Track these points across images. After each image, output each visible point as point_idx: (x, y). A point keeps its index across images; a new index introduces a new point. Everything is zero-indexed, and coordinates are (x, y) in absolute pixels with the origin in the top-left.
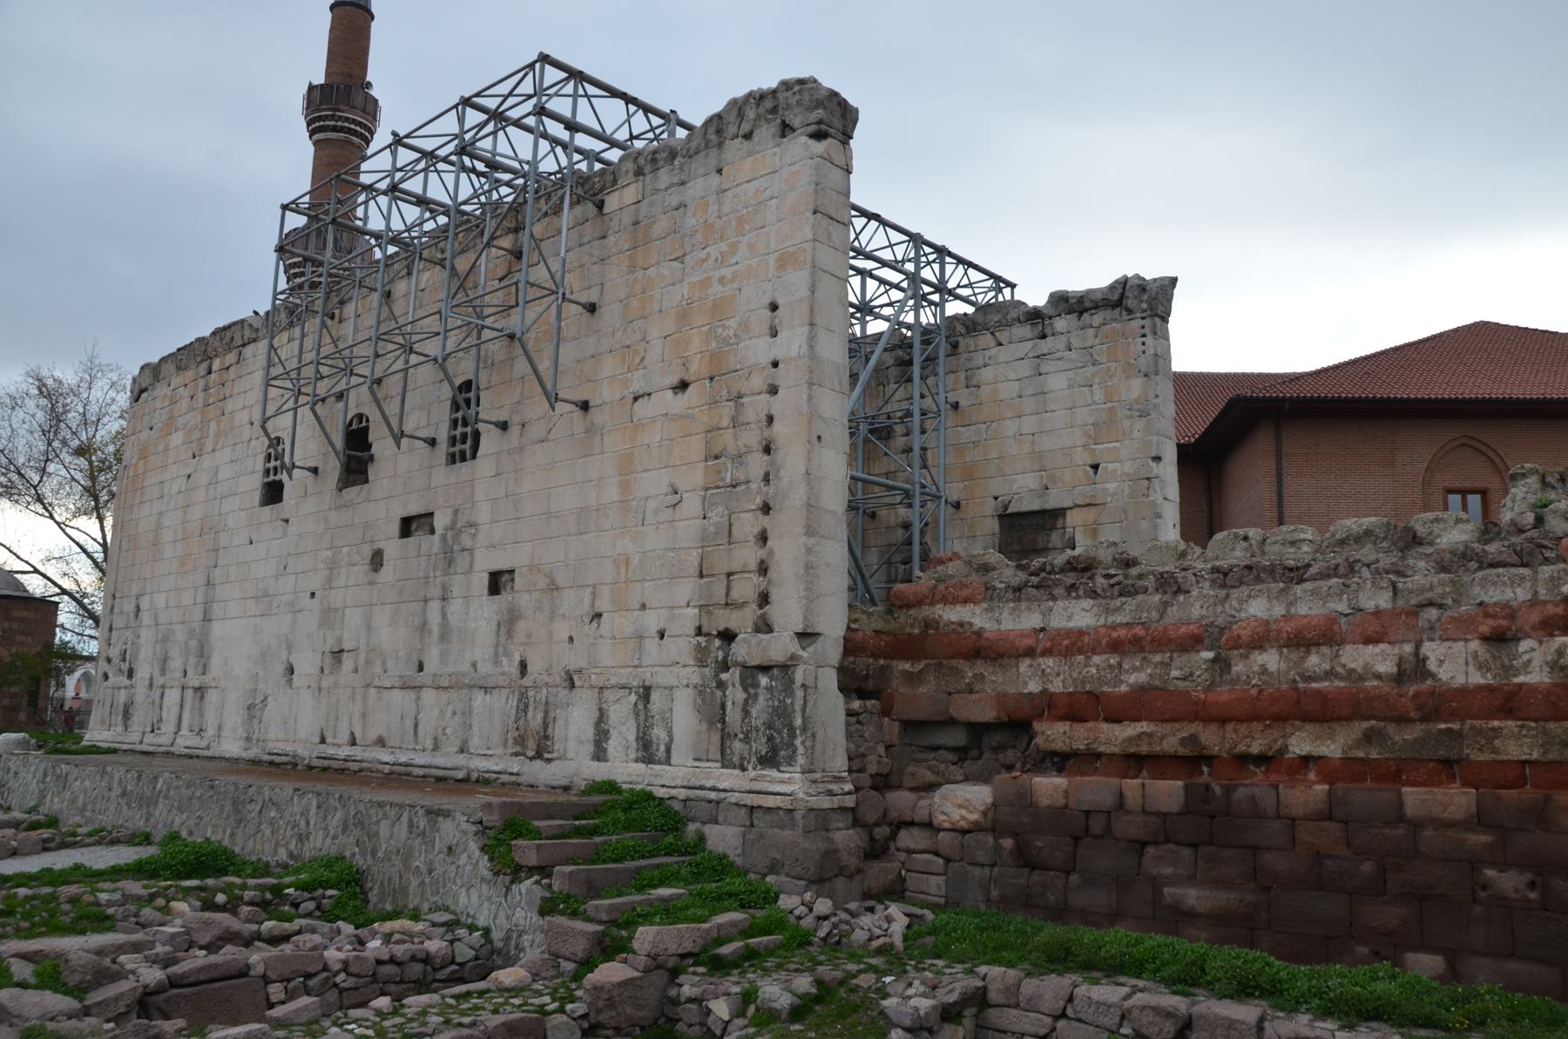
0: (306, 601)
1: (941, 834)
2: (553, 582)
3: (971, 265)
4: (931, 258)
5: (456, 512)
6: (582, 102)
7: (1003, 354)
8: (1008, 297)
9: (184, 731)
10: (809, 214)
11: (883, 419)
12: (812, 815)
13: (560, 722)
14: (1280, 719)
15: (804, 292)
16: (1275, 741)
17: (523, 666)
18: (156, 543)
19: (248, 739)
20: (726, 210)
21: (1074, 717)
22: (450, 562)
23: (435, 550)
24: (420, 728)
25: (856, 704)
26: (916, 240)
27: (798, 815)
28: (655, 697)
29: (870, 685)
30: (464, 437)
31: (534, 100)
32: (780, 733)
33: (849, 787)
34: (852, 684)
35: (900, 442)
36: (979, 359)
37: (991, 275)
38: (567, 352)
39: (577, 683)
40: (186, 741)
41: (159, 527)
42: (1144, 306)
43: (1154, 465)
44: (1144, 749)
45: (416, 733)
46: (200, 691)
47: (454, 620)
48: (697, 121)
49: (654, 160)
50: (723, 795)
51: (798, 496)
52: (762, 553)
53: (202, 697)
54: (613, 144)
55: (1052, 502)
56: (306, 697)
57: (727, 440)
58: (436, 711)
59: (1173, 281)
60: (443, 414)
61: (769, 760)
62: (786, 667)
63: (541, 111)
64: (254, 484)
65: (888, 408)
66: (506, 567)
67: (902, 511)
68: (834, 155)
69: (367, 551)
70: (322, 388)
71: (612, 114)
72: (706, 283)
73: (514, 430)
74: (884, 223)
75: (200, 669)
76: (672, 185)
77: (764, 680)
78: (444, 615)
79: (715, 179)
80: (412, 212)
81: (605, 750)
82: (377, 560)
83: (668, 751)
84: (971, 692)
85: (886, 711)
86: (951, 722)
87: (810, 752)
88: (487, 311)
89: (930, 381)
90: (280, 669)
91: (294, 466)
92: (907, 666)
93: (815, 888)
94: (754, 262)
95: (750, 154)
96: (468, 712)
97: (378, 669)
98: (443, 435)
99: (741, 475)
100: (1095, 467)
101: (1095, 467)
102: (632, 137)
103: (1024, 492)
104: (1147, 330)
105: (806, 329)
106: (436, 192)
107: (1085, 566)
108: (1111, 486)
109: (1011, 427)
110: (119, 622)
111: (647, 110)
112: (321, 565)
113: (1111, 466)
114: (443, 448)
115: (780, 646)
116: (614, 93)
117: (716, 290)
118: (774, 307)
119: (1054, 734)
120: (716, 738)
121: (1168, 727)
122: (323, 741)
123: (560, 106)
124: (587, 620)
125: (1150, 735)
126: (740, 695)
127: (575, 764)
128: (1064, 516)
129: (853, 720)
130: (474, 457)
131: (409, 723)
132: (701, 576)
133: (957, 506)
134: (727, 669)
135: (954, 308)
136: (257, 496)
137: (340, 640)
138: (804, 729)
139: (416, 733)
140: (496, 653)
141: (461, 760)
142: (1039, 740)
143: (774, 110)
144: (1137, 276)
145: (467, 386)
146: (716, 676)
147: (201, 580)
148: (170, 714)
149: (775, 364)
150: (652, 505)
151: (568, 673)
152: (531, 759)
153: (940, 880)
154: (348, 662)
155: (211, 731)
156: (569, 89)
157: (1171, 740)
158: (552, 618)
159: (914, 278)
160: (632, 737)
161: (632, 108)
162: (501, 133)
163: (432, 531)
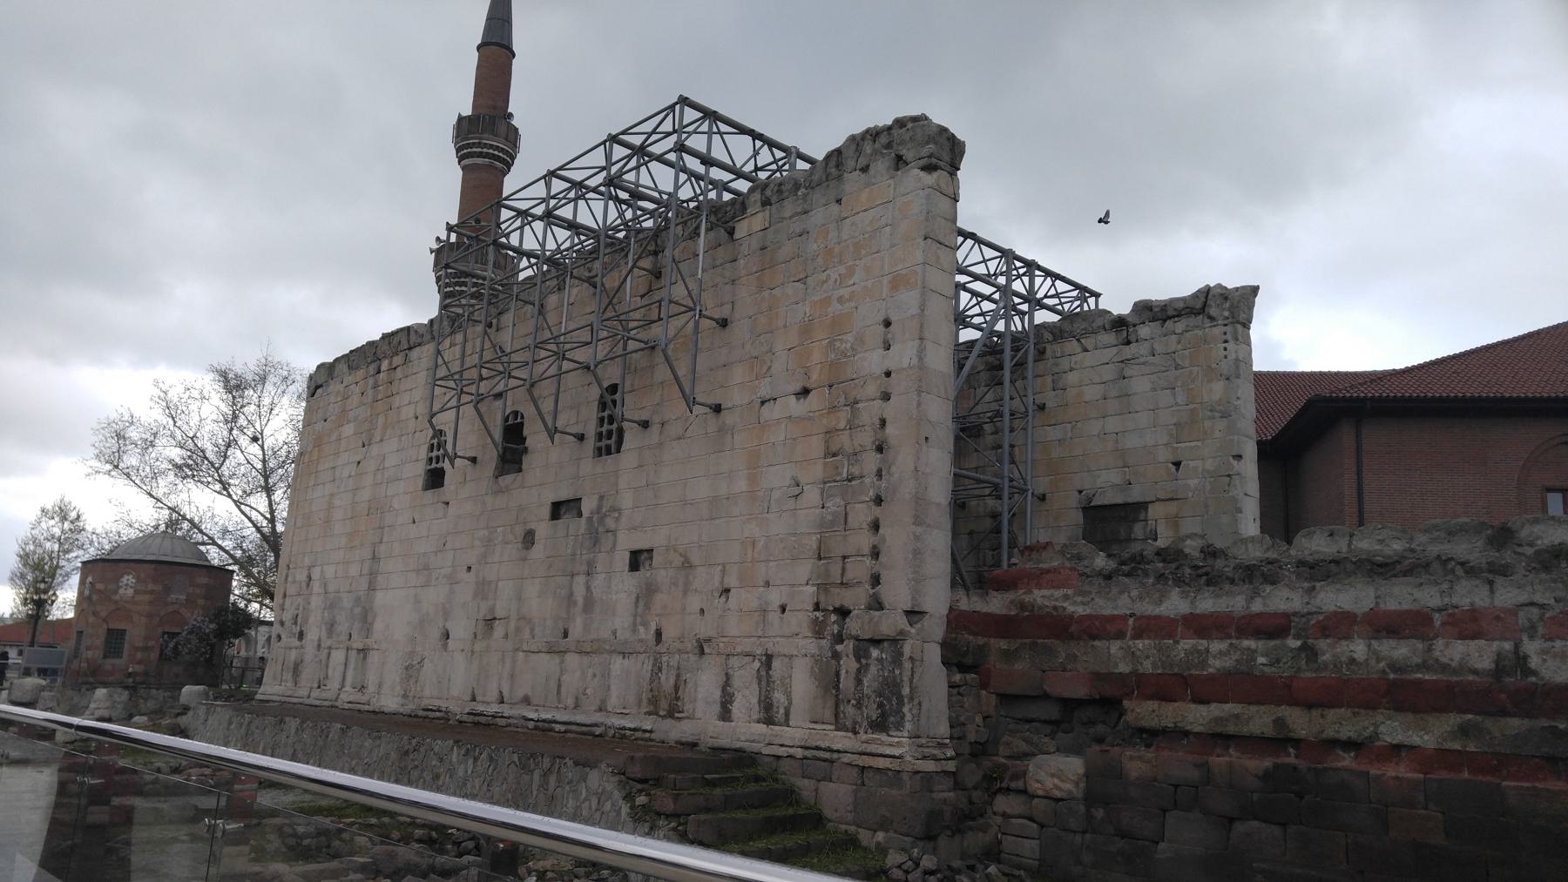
0: (463, 575)
1: (1036, 800)
2: (687, 560)
3: (1057, 277)
4: (1022, 271)
5: (601, 498)
6: (716, 138)
7: (1089, 359)
8: (1093, 307)
9: (348, 688)
10: (920, 240)
11: (972, 419)
12: (918, 777)
13: (690, 685)
14: (1371, 706)
15: (915, 310)
16: (1365, 728)
17: (659, 634)
18: (327, 521)
19: (405, 696)
20: (844, 236)
21: (1165, 697)
22: (596, 542)
23: (582, 531)
24: (563, 689)
25: (957, 677)
26: (1007, 255)
27: (905, 777)
28: (776, 664)
29: (969, 660)
30: (610, 433)
31: (674, 138)
32: (889, 701)
33: (950, 753)
34: (956, 659)
35: (989, 439)
36: (1065, 364)
37: (1076, 286)
38: (703, 361)
39: (707, 650)
40: (348, 695)
41: (330, 507)
42: (1226, 314)
43: (1235, 463)
44: (1231, 729)
45: (559, 692)
46: (364, 652)
47: (597, 593)
48: (819, 156)
49: (780, 192)
50: (835, 756)
51: (907, 490)
52: (873, 540)
54: (739, 175)
55: (1135, 495)
57: (844, 441)
58: (578, 674)
59: (1255, 290)
60: (591, 413)
61: (880, 725)
62: (896, 641)
63: (681, 148)
64: (420, 469)
65: (979, 409)
67: (991, 502)
68: (943, 186)
69: (520, 531)
70: (484, 387)
71: (741, 148)
72: (826, 301)
73: (655, 429)
74: (979, 241)
76: (797, 214)
77: (875, 653)
78: (588, 589)
79: (834, 208)
80: (562, 234)
81: (729, 711)
82: (529, 539)
83: (787, 714)
84: (1064, 670)
85: (984, 685)
86: (1045, 696)
87: (917, 718)
88: (632, 325)
89: (1019, 384)
90: (436, 634)
91: (456, 456)
92: (1003, 644)
93: (921, 844)
94: (869, 284)
95: (868, 185)
96: (606, 674)
97: (526, 634)
98: (591, 430)
99: (856, 471)
100: (1177, 464)
101: (1177, 464)
102: (757, 169)
103: (1107, 485)
104: (1229, 337)
105: (917, 342)
106: (584, 218)
107: (1170, 555)
108: (1193, 482)
109: (1095, 427)
110: (292, 590)
111: (772, 144)
112: (477, 543)
113: (1192, 464)
114: (590, 443)
115: (892, 622)
116: (742, 130)
117: (835, 308)
118: (887, 324)
119: (1143, 712)
120: (831, 703)
121: (1254, 708)
122: (474, 699)
123: (697, 143)
124: (717, 594)
125: (1237, 716)
126: (854, 665)
127: (702, 723)
128: (1146, 509)
129: (955, 691)
130: (618, 451)
131: (553, 685)
132: (820, 558)
133: (1043, 498)
134: (842, 641)
135: (1042, 316)
136: (420, 482)
137: (492, 609)
138: (911, 699)
139: (559, 692)
140: (635, 624)
141: (598, 718)
142: (1129, 717)
143: (889, 146)
144: (1219, 286)
145: (613, 389)
146: (832, 647)
147: (367, 553)
148: (335, 672)
149: (888, 374)
150: (776, 495)
151: (698, 641)
152: (663, 717)
153: (1035, 843)
154: (499, 630)
155: (371, 688)
156: (705, 127)
157: (1259, 720)
158: (685, 592)
159: (1006, 291)
160: (755, 700)
161: (758, 143)
162: (643, 169)
163: (580, 515)
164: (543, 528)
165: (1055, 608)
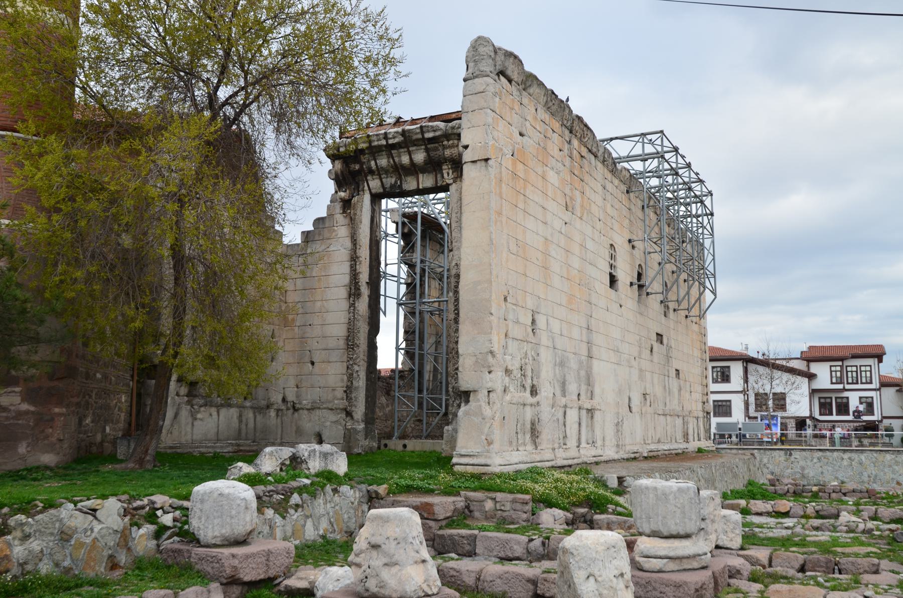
9: (583, 445)
19: (618, 446)
53: (592, 417)
56: (638, 417)
75: (589, 395)
148: (572, 430)
155: (599, 443)
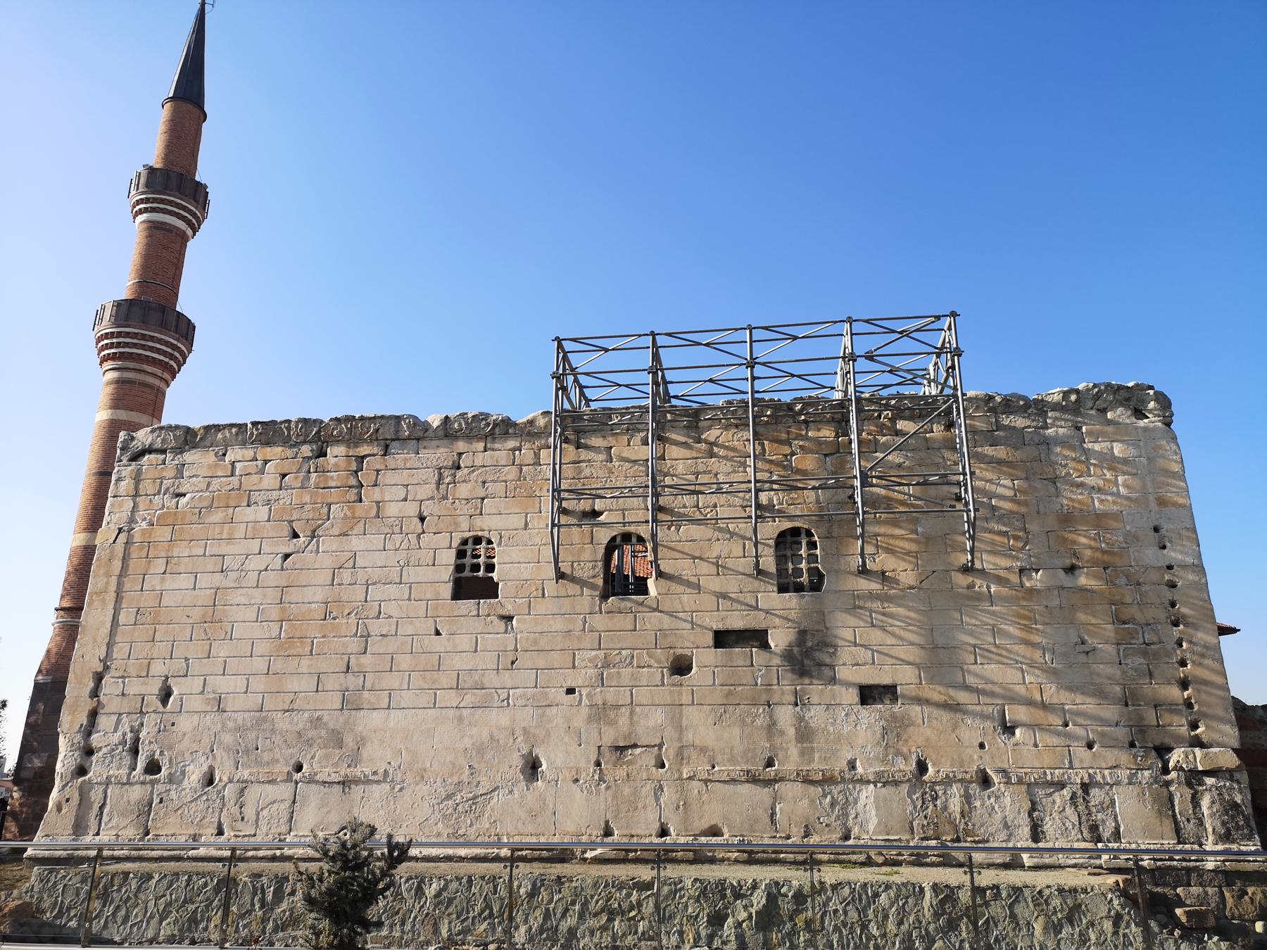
45: (773, 821)
66: (886, 680)
77: (1210, 781)
82: (681, 667)
126: (1188, 793)
139: (773, 821)
143: (1128, 400)
164: (705, 658)
165: (1254, 745)
